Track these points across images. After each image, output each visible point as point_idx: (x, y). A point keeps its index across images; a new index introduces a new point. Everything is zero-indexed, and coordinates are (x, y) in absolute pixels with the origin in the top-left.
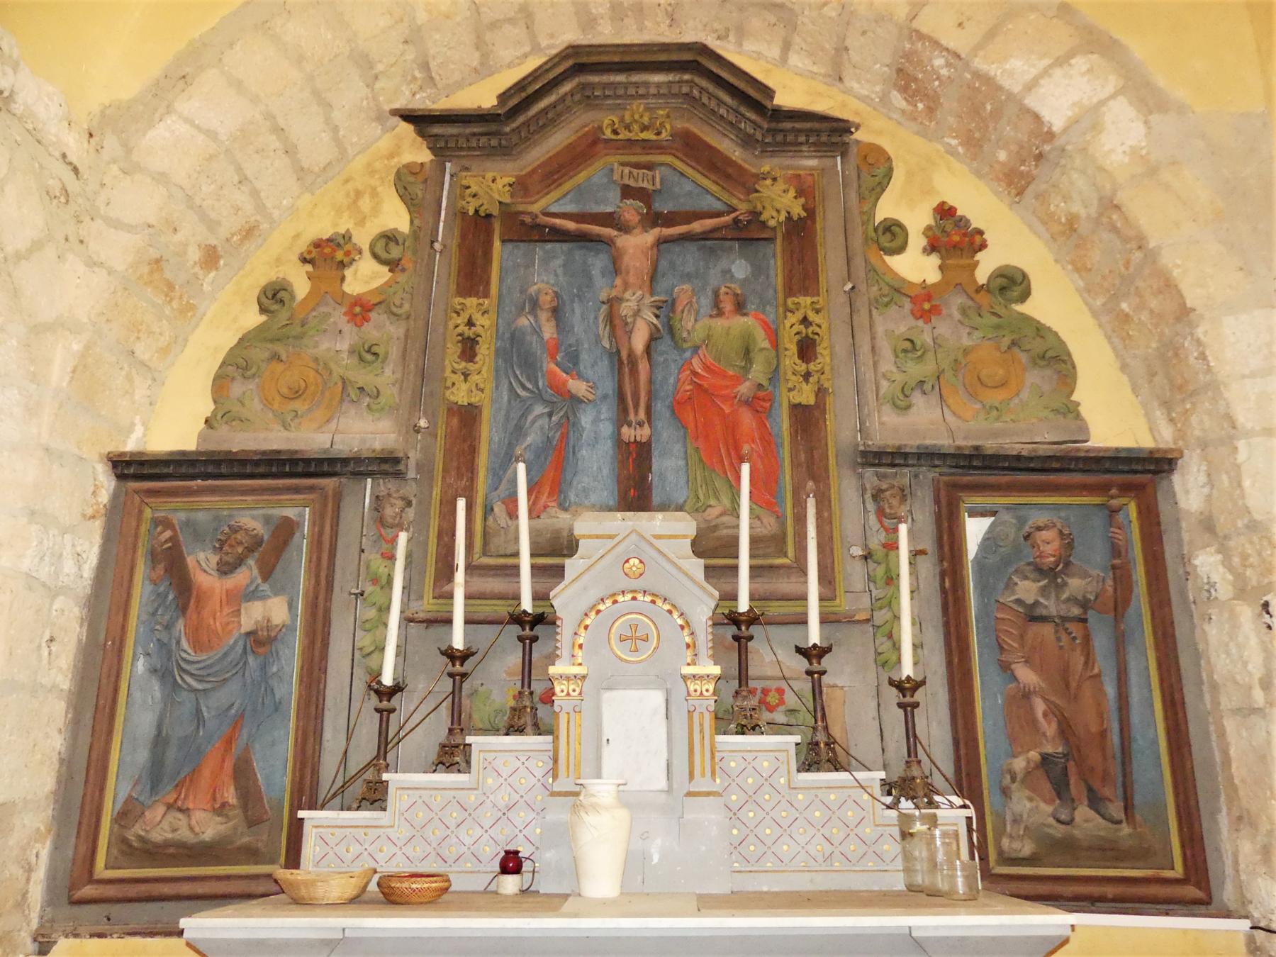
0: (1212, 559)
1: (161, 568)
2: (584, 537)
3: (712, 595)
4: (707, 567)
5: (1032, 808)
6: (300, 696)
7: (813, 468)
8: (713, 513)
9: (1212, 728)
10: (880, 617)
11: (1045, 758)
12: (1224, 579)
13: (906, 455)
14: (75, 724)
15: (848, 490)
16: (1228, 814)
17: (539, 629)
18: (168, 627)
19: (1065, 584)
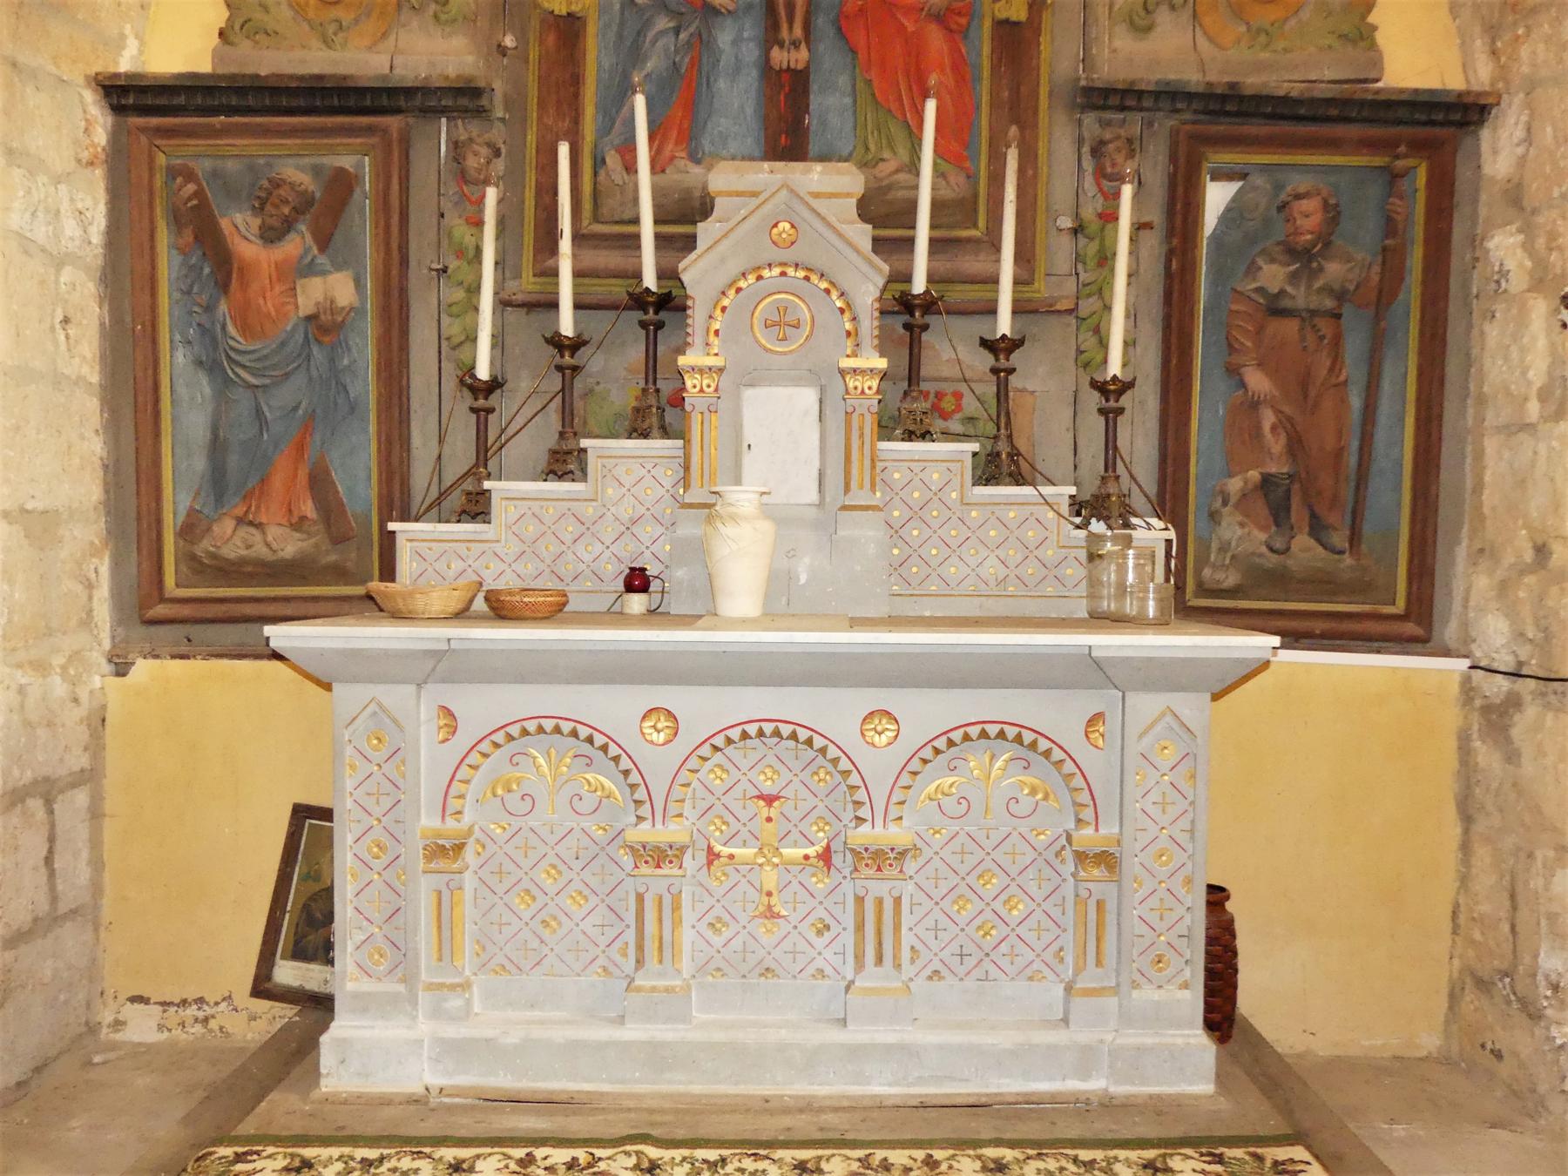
0: (1512, 240)
1: (188, 235)
2: (720, 193)
3: (880, 270)
4: (875, 240)
5: (1242, 535)
6: (380, 394)
7: (1018, 110)
8: (885, 169)
9: (1469, 448)
10: (1087, 306)
11: (1267, 481)
12: (1521, 265)
13: (1140, 94)
14: (112, 427)
15: (1060, 141)
16: (1469, 547)
17: (663, 315)
18: (209, 309)
19: (1321, 269)
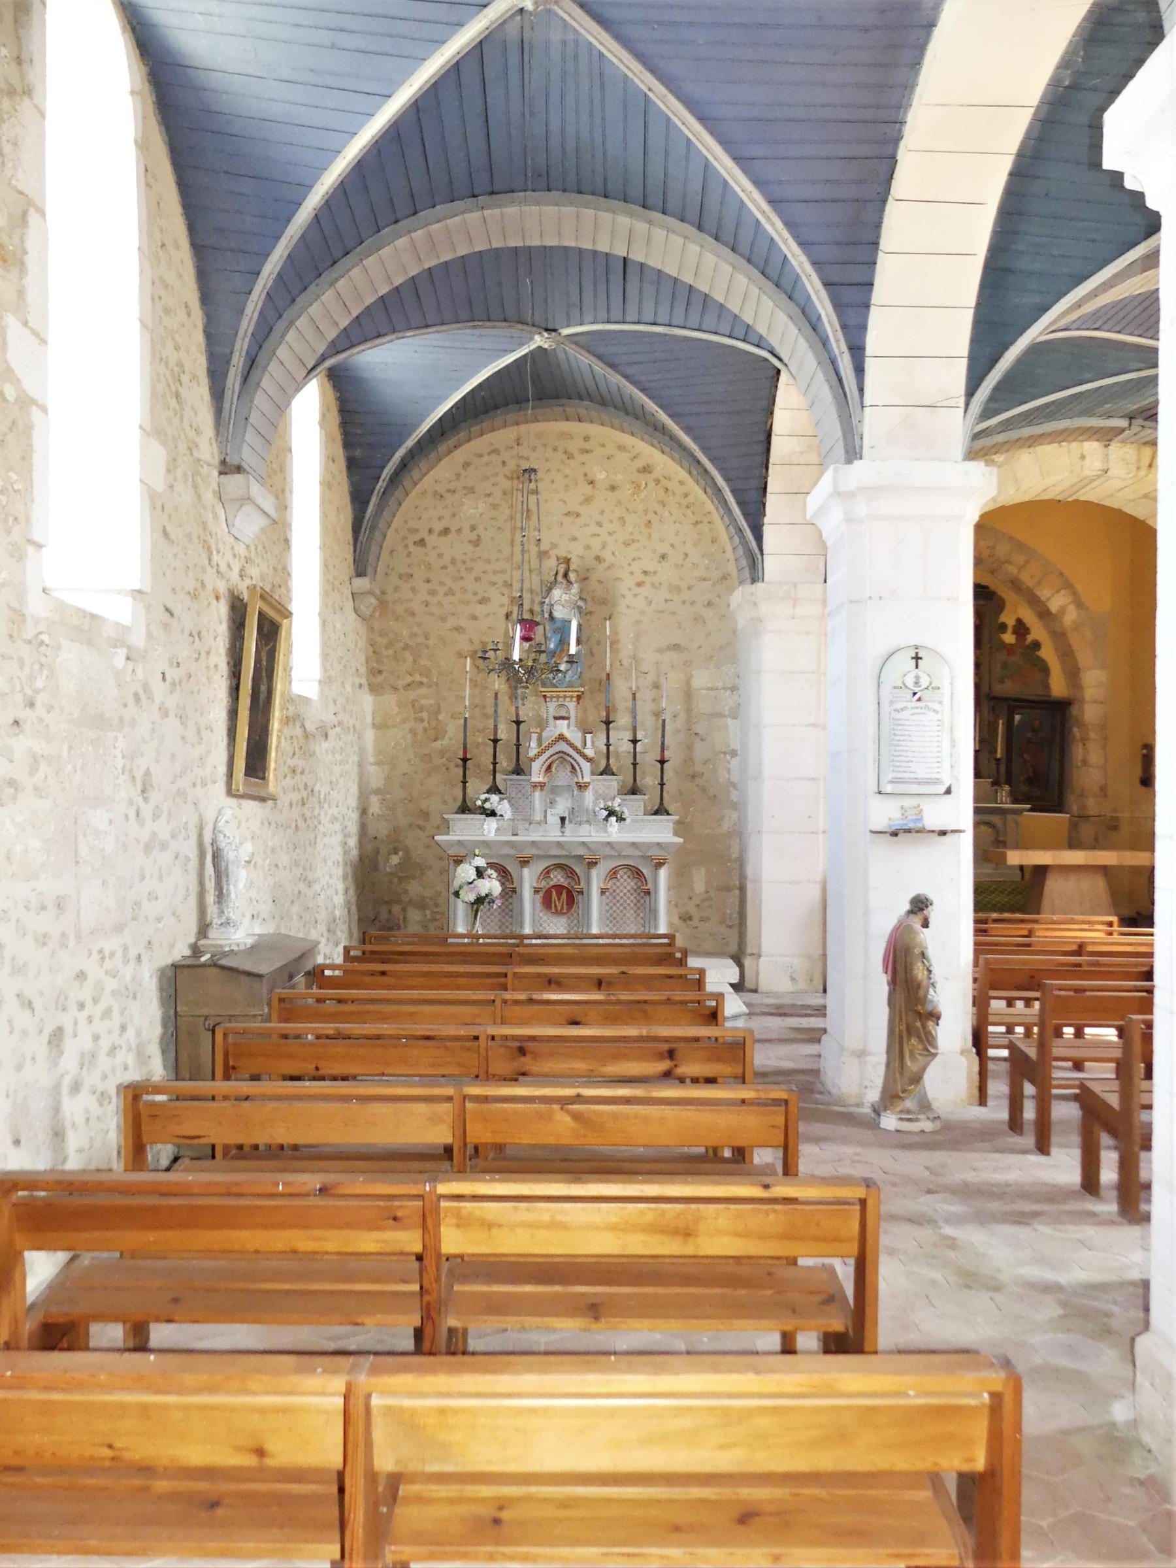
5: (1024, 788)
